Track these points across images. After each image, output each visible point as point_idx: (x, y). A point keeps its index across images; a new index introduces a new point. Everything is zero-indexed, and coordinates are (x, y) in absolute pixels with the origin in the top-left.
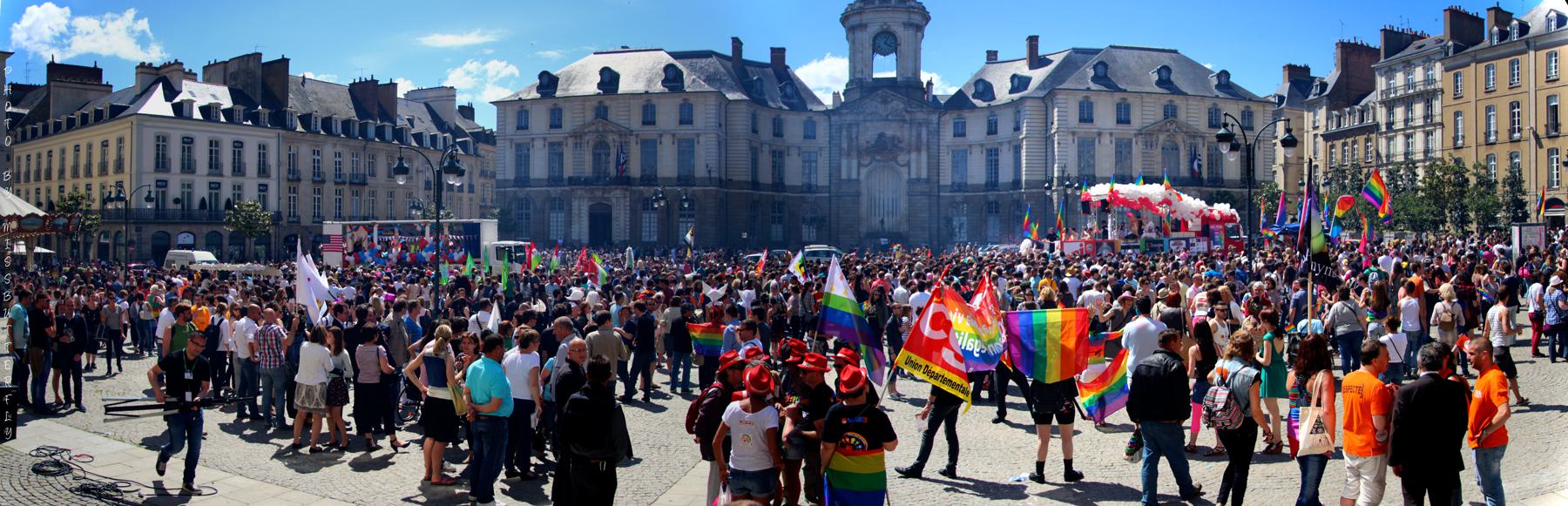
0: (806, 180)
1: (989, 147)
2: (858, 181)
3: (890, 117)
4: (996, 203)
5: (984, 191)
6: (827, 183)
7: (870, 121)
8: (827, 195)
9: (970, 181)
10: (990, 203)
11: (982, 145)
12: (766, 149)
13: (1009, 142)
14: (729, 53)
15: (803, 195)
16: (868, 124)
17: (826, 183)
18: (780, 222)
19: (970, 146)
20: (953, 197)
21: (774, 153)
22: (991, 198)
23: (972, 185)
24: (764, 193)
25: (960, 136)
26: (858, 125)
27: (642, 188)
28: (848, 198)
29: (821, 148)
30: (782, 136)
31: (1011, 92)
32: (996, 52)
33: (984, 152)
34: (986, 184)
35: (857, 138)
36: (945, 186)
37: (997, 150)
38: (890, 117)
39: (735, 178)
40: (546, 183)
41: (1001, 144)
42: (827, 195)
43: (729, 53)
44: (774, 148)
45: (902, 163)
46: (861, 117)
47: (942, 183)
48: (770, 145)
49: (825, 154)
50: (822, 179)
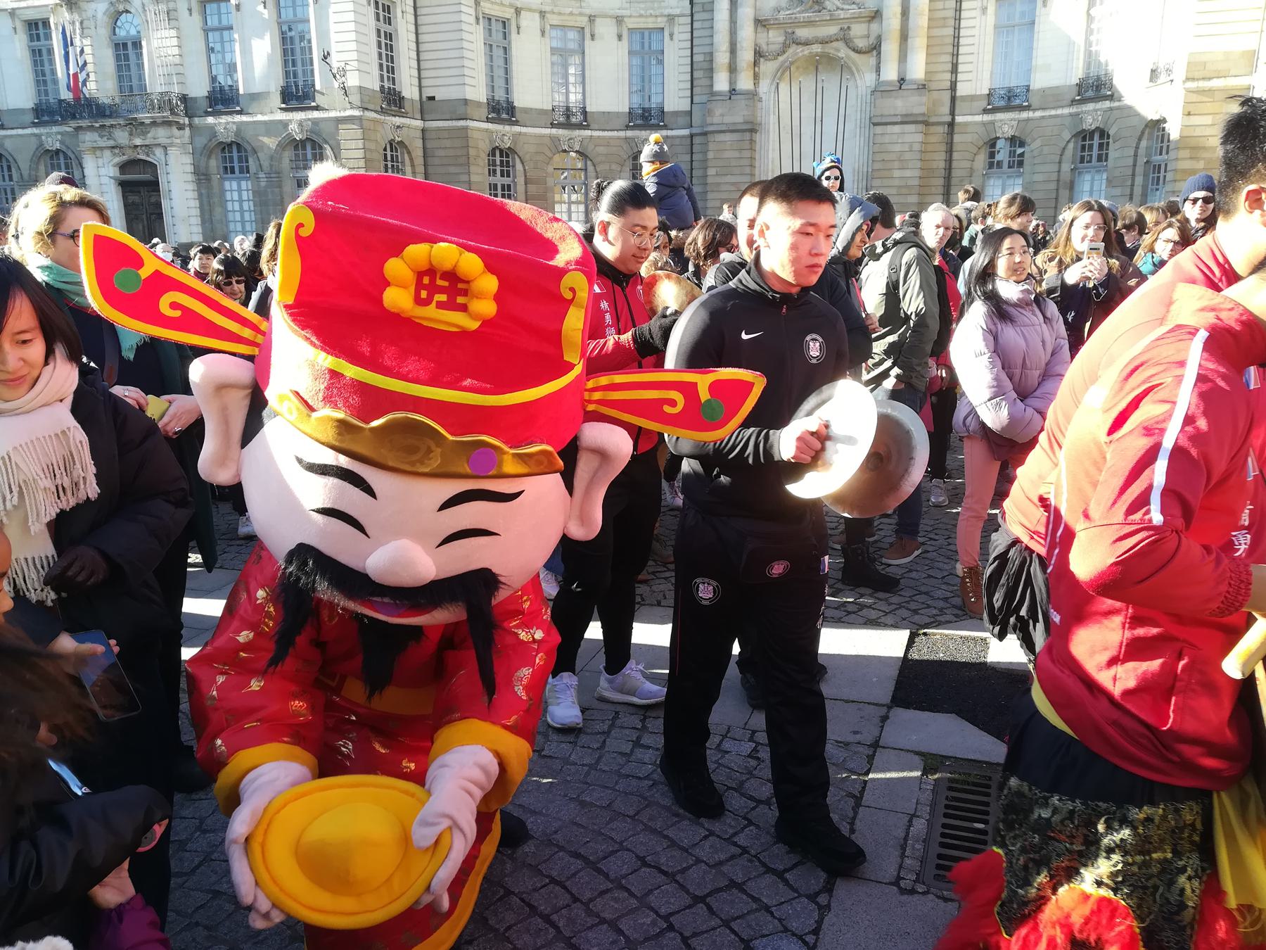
0: (637, 100)
2: (753, 95)
4: (1103, 133)
6: (684, 105)
8: (686, 132)
9: (1039, 81)
10: (1084, 136)
15: (630, 133)
17: (684, 105)
20: (993, 123)
22: (1090, 123)
24: (524, 130)
27: (210, 120)
28: (728, 137)
29: (671, 18)
36: (972, 98)
40: (30, 118)
42: (686, 132)
45: (861, 43)
47: (962, 90)
48: (542, 14)
49: (681, 32)
50: (674, 98)
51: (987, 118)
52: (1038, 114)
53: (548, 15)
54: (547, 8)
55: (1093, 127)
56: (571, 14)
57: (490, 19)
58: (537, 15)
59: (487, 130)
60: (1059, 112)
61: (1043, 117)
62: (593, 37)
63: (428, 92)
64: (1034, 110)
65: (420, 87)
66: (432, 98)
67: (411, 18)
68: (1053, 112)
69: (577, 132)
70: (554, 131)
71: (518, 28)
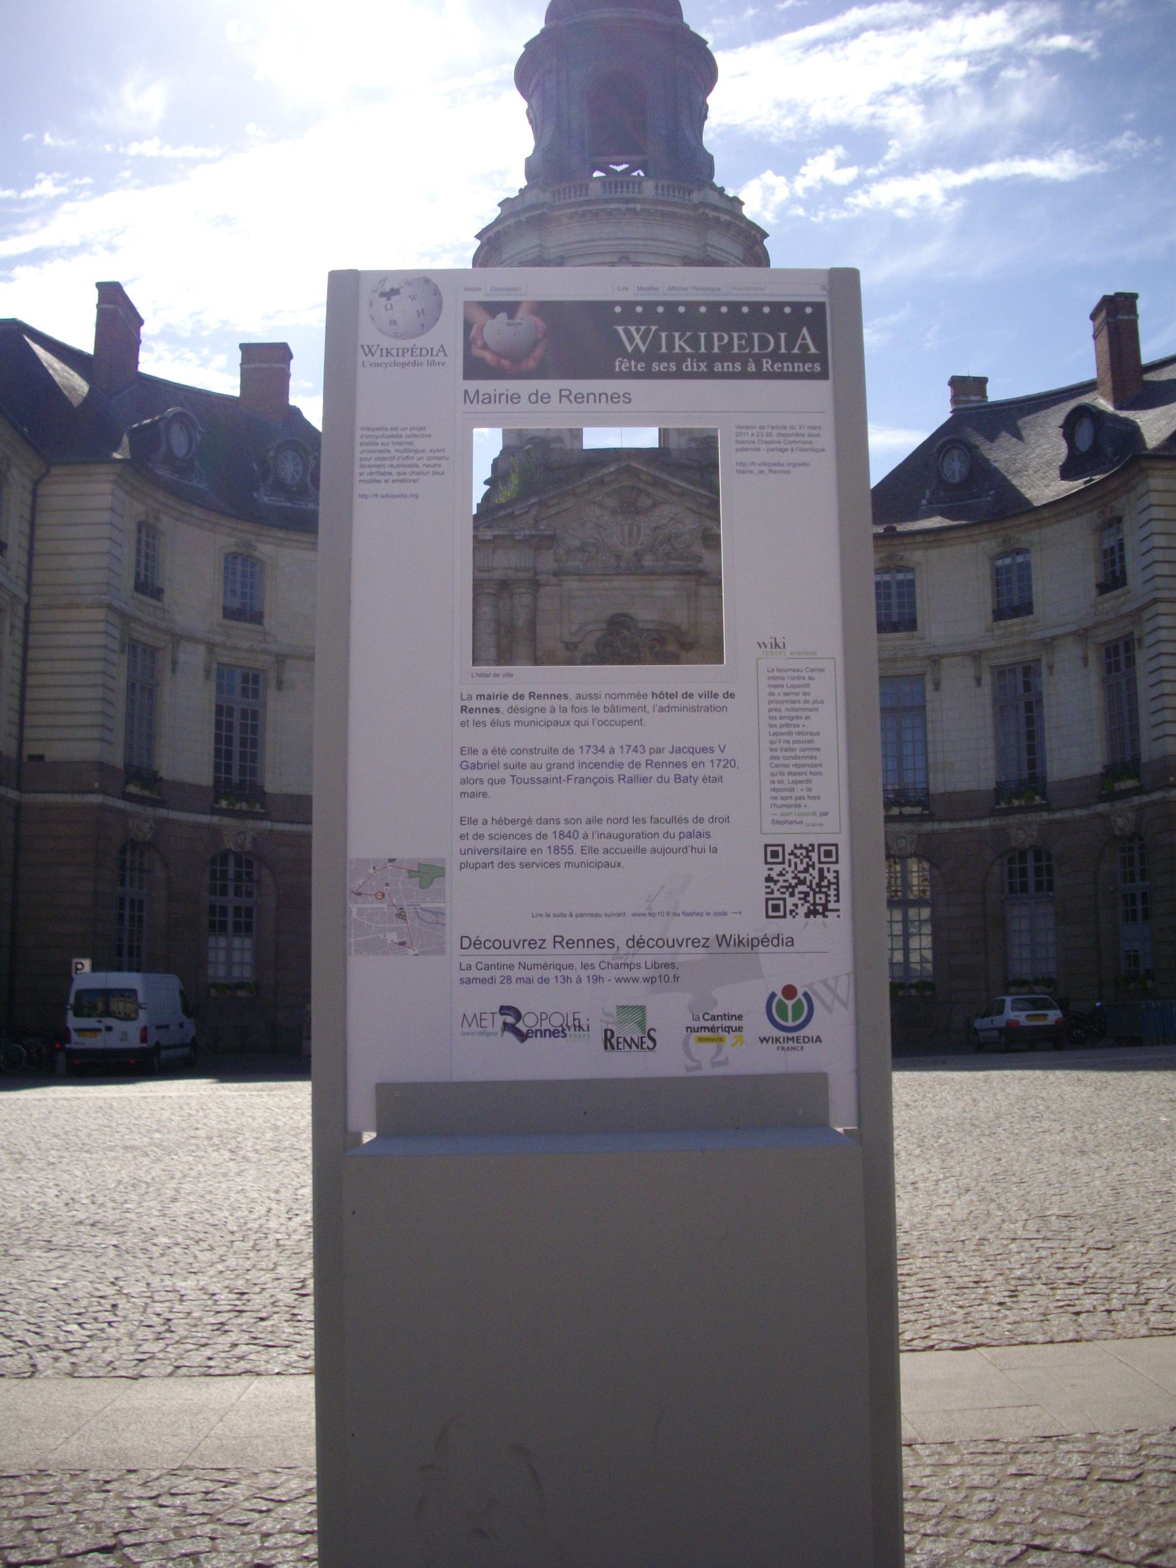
1: (1004, 659)
3: (648, 561)
5: (993, 813)
7: (576, 573)
9: (939, 784)
11: (976, 656)
12: (193, 658)
13: (1082, 635)
14: (84, 340)
16: (572, 584)
18: (244, 928)
19: (935, 660)
21: (222, 675)
23: (948, 796)
24: (173, 815)
25: (895, 627)
26: (535, 585)
30: (257, 618)
31: (1067, 472)
32: (981, 382)
33: (987, 679)
34: (1000, 791)
35: (533, 624)
37: (1029, 671)
38: (648, 561)
39: (56, 752)
41: (1049, 644)
43: (84, 340)
44: (224, 657)
46: (547, 561)
48: (211, 647)
51: (997, 822)
52: (946, 826)
53: (218, 650)
54: (218, 639)
55: (1027, 845)
56: (251, 650)
57: (134, 648)
58: (202, 649)
59: (121, 812)
60: (976, 824)
61: (953, 831)
62: (280, 685)
63: (32, 749)
64: (941, 821)
65: (21, 740)
66: (41, 758)
67: (18, 636)
68: (967, 824)
69: (251, 824)
70: (215, 819)
71: (175, 663)
